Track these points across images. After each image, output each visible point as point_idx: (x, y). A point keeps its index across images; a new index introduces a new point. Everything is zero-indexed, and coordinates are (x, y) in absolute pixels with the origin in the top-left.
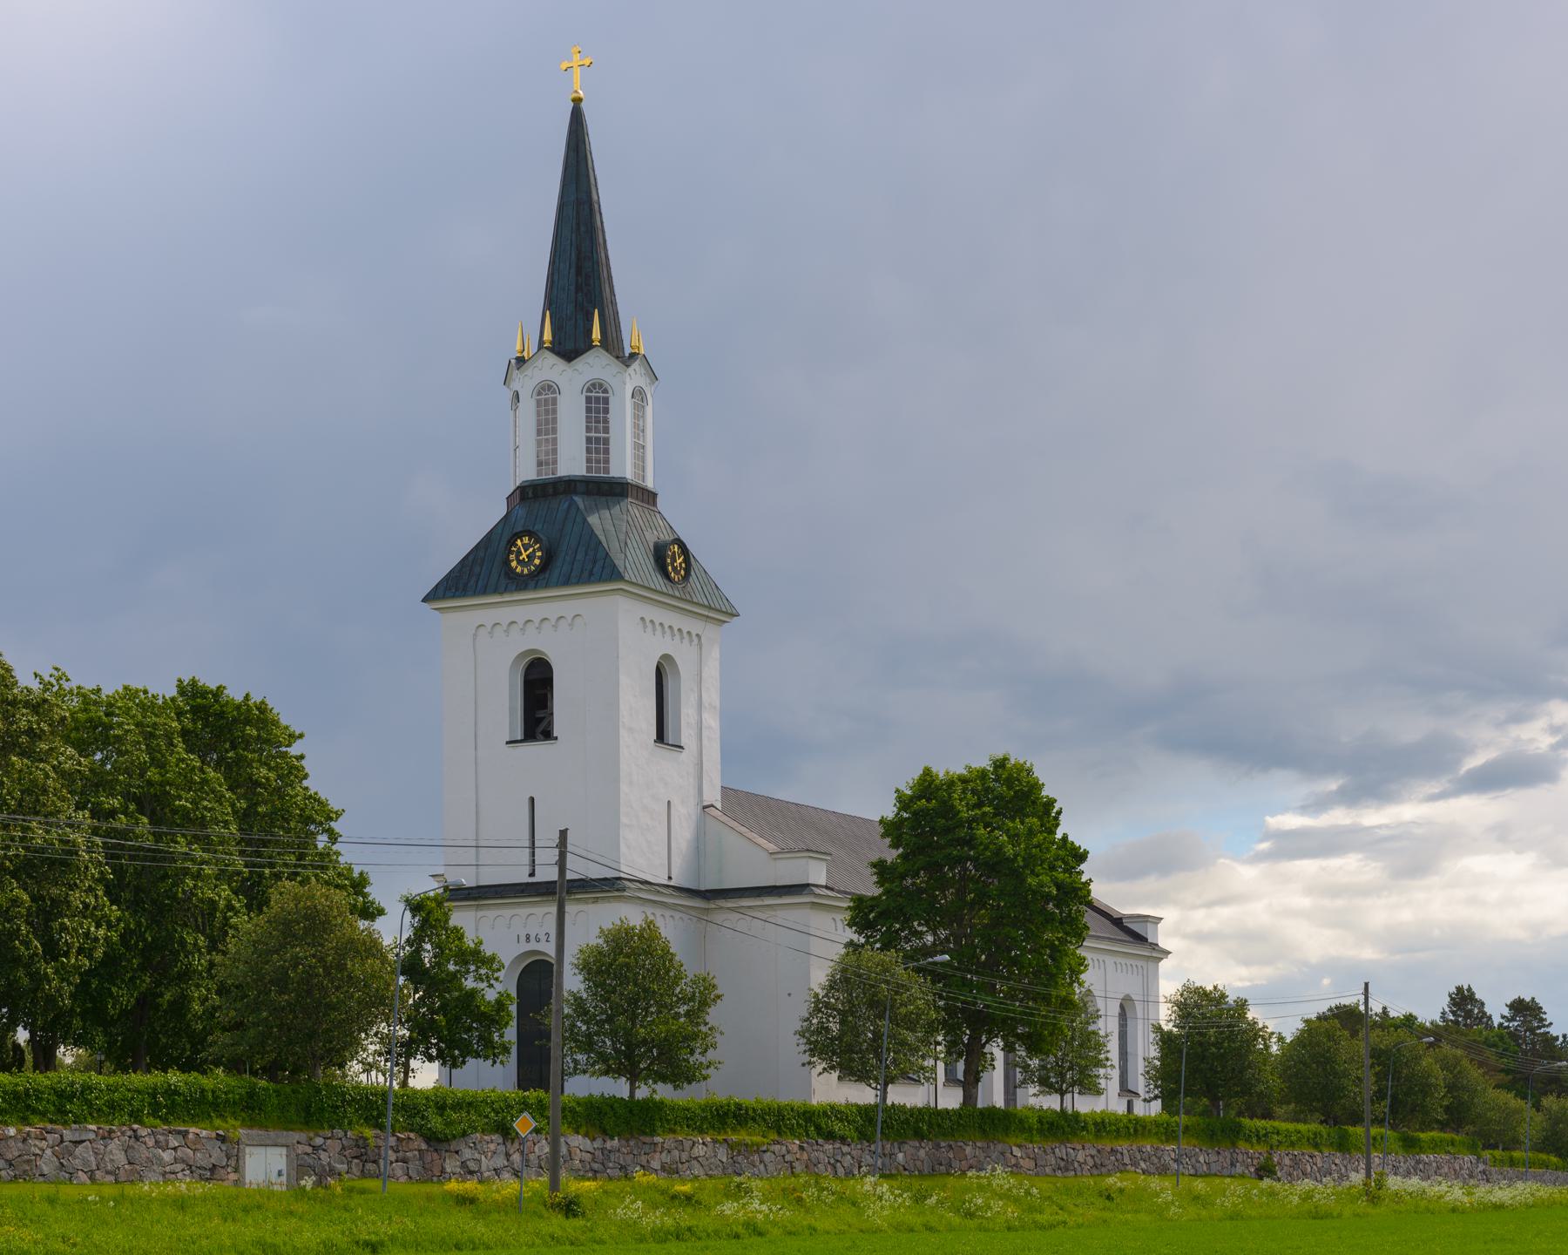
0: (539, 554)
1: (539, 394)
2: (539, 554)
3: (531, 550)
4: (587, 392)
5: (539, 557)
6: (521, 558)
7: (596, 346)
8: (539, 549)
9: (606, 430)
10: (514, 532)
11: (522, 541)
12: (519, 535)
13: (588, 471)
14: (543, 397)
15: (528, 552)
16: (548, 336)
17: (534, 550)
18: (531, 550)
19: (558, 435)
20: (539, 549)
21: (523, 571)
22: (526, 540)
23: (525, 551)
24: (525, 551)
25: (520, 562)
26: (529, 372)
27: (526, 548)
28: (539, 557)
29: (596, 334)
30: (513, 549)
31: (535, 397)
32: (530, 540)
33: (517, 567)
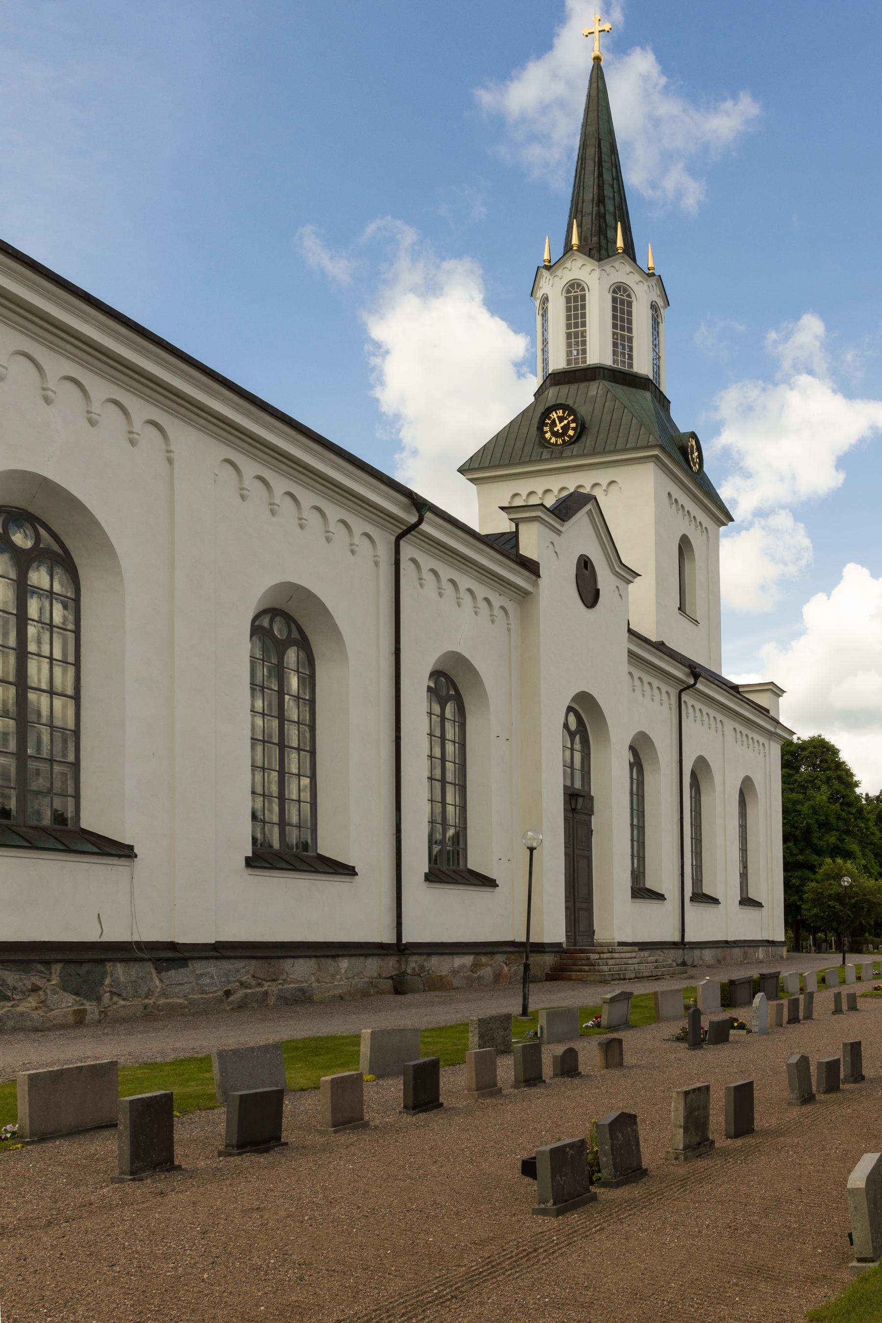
0: (573, 425)
1: (568, 292)
2: (573, 425)
3: (566, 422)
4: (613, 293)
5: (573, 429)
6: (555, 429)
7: (619, 253)
8: (573, 421)
9: (630, 330)
10: (546, 407)
11: (557, 414)
12: (555, 408)
13: (615, 361)
14: (572, 294)
15: (562, 424)
16: (575, 240)
17: (569, 422)
18: (566, 422)
19: (587, 328)
20: (573, 421)
21: (556, 441)
22: (560, 413)
23: (560, 423)
24: (560, 423)
25: (555, 434)
26: (559, 273)
27: (561, 419)
28: (573, 429)
29: (620, 243)
30: (547, 421)
31: (564, 294)
32: (564, 413)
33: (551, 438)
